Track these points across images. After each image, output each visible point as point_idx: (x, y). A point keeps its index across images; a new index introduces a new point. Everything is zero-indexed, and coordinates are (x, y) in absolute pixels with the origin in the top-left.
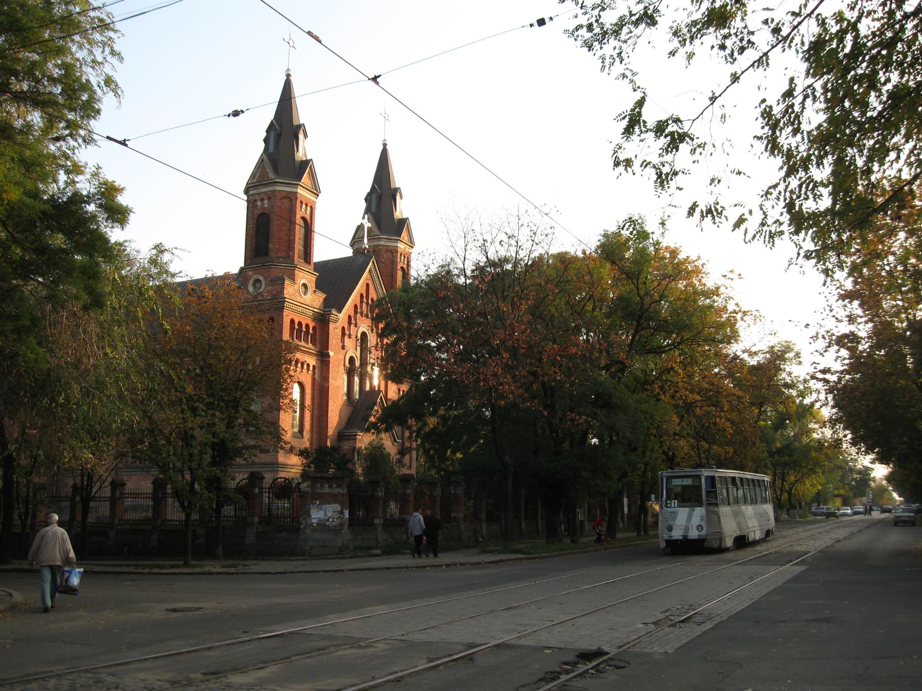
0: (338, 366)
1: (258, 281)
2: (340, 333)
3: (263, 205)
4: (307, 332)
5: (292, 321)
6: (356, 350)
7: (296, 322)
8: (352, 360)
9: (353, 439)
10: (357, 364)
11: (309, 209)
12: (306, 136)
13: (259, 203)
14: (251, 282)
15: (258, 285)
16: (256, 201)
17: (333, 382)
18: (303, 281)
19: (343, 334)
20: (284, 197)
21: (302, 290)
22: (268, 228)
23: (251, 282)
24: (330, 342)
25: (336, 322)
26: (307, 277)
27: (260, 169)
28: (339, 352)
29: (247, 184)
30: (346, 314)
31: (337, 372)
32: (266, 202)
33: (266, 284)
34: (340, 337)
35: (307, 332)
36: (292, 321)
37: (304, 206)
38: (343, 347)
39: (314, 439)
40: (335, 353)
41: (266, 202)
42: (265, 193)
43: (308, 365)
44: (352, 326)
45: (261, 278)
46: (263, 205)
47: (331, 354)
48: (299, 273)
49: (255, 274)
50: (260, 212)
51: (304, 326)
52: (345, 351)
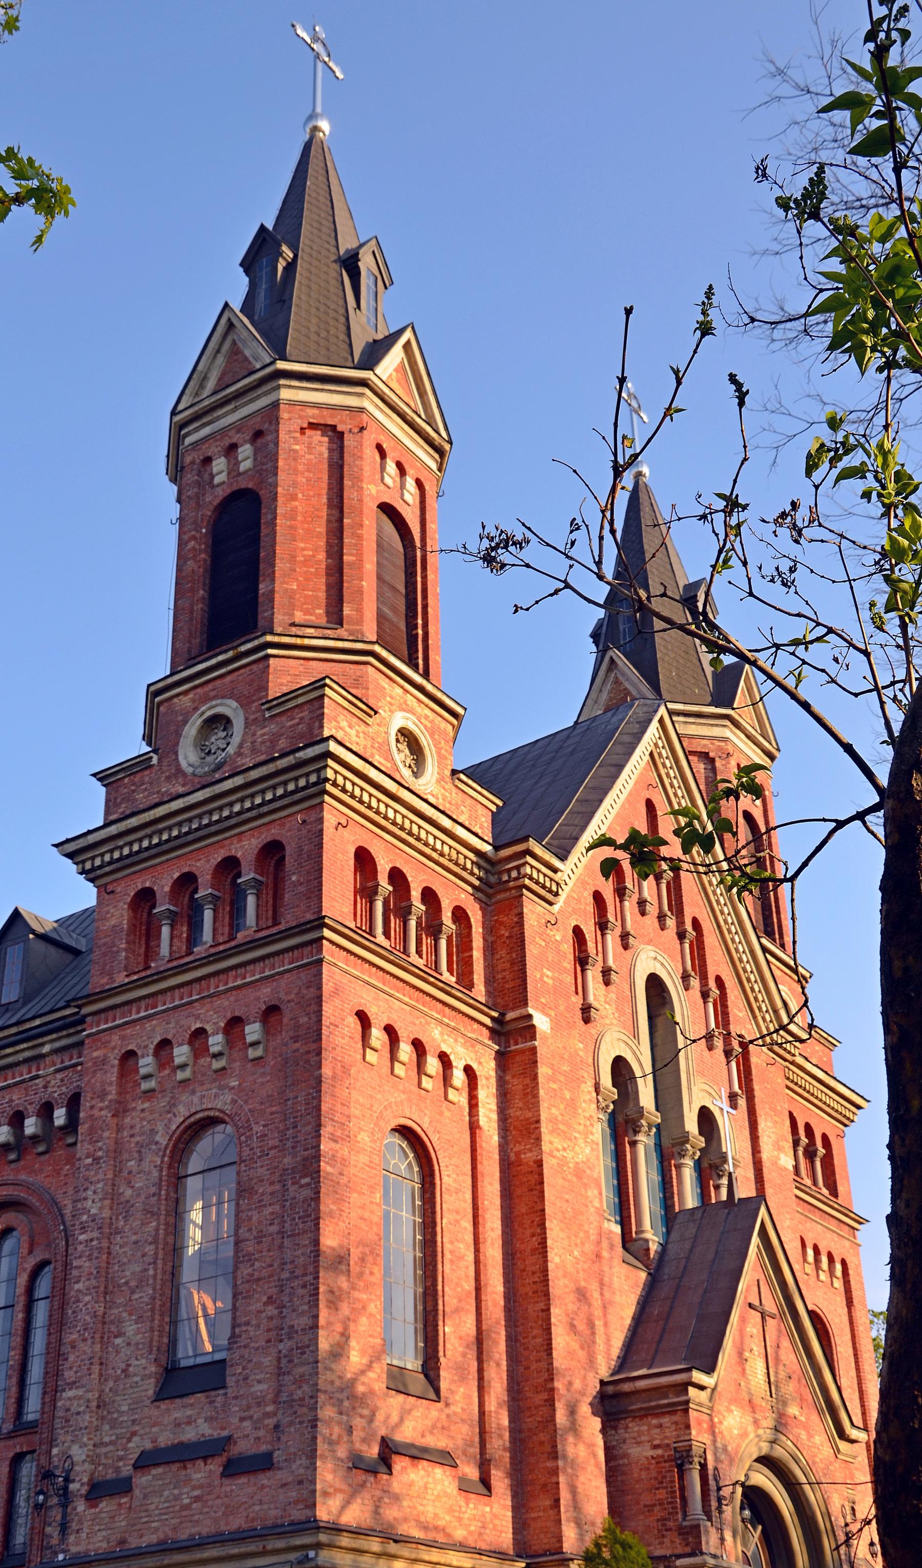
0: (574, 1081)
1: (219, 722)
2: (568, 948)
3: (234, 464)
4: (432, 927)
5: (364, 859)
6: (636, 1035)
7: (383, 866)
8: (620, 1066)
9: (671, 1409)
10: (646, 1096)
11: (410, 484)
12: (385, 280)
13: (219, 465)
14: (191, 730)
15: (217, 738)
16: (208, 460)
17: (557, 1143)
18: (399, 720)
19: (582, 961)
20: (312, 426)
21: (401, 756)
22: (256, 539)
23: (191, 730)
24: (533, 973)
25: (549, 895)
26: (420, 710)
27: (220, 359)
28: (571, 1026)
29: (174, 413)
30: (582, 883)
31: (572, 1105)
32: (245, 451)
33: (247, 724)
34: (568, 963)
35: (432, 927)
36: (364, 859)
37: (391, 467)
38: (586, 1012)
39: (492, 1405)
40: (556, 1025)
41: (245, 451)
42: (238, 427)
43: (444, 1058)
44: (612, 939)
45: (229, 708)
46: (234, 464)
47: (541, 1022)
48: (384, 682)
49: (206, 699)
50: (221, 493)
51: (416, 895)
52: (592, 1029)
